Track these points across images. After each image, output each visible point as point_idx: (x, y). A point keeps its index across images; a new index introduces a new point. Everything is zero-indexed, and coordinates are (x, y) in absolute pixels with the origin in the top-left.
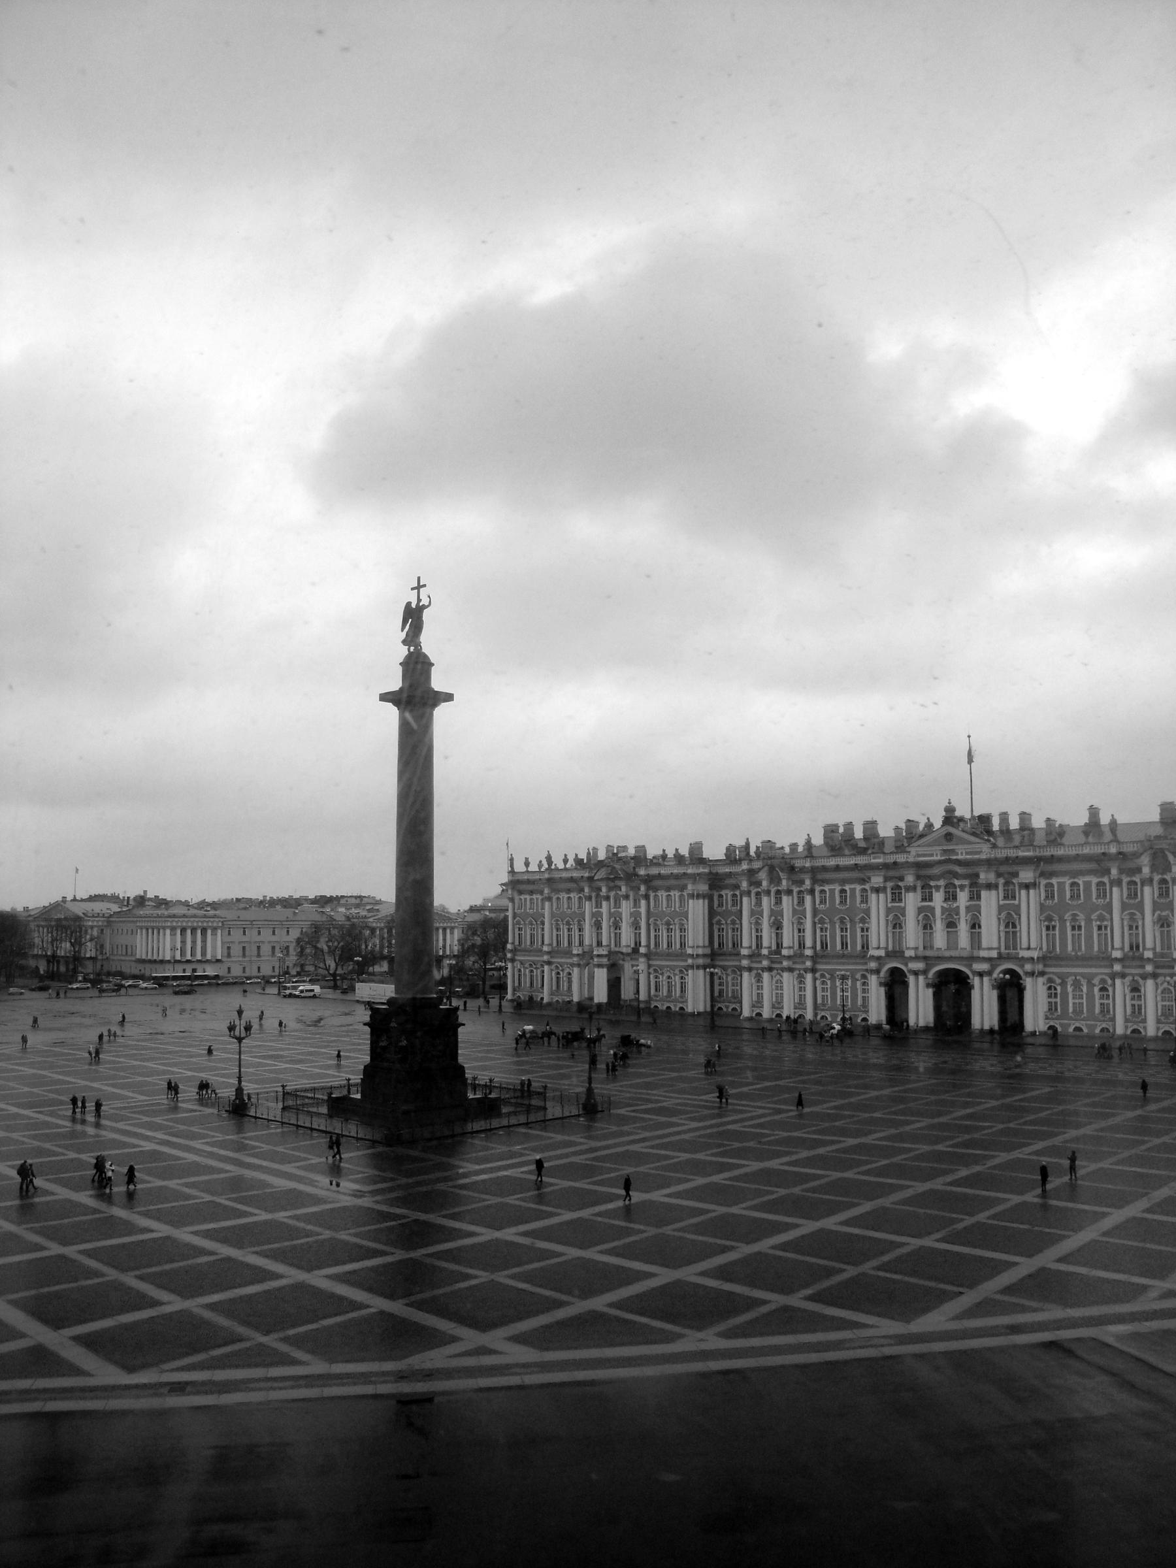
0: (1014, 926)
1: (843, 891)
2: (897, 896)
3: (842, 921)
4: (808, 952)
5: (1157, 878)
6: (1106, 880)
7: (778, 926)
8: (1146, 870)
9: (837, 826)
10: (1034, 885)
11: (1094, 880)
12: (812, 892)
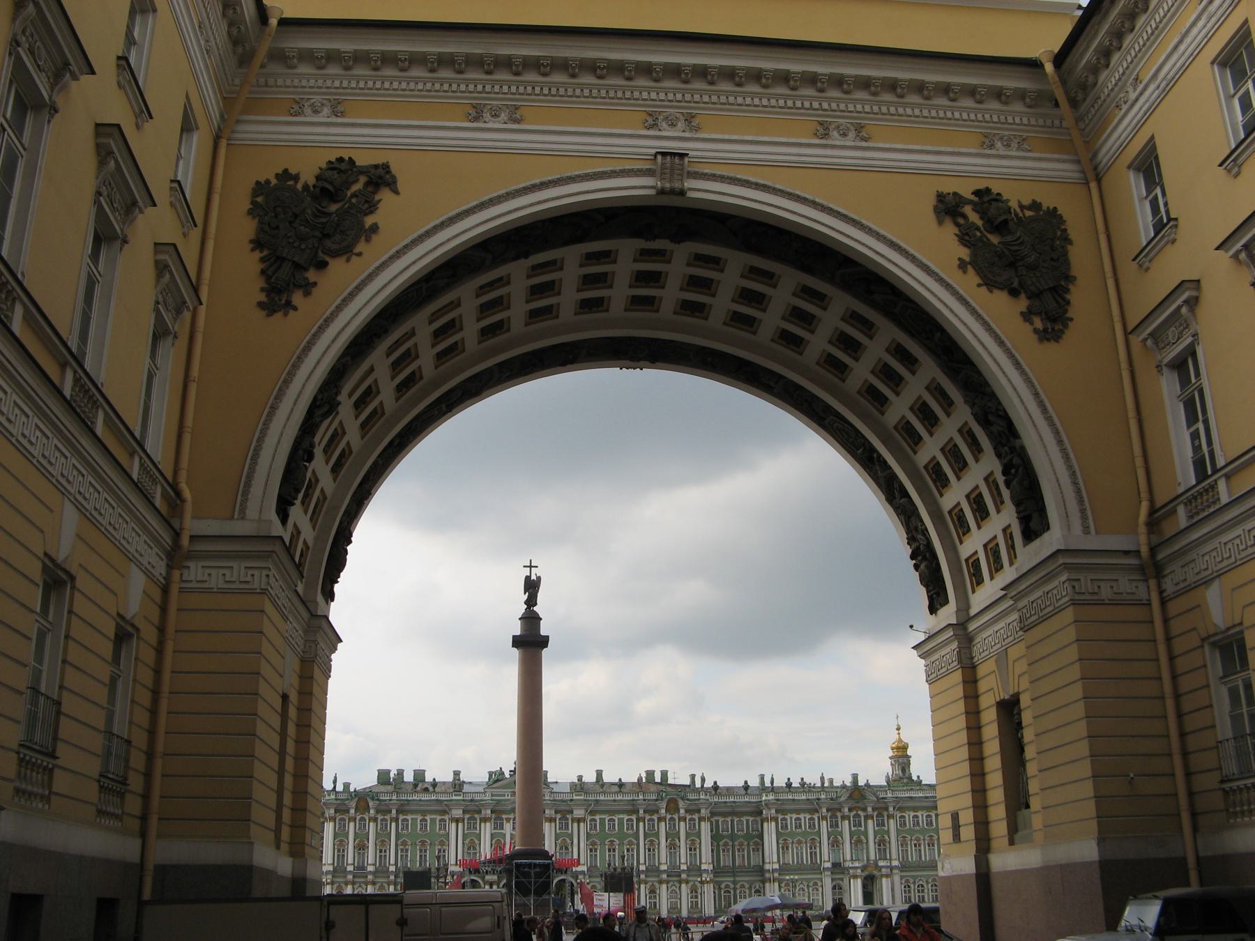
0: (567, 848)
1: (424, 820)
2: (472, 825)
3: (423, 843)
4: (392, 868)
5: (669, 816)
6: (634, 817)
7: (361, 848)
8: (663, 811)
9: (389, 771)
10: (584, 820)
11: (626, 817)
12: (397, 820)
